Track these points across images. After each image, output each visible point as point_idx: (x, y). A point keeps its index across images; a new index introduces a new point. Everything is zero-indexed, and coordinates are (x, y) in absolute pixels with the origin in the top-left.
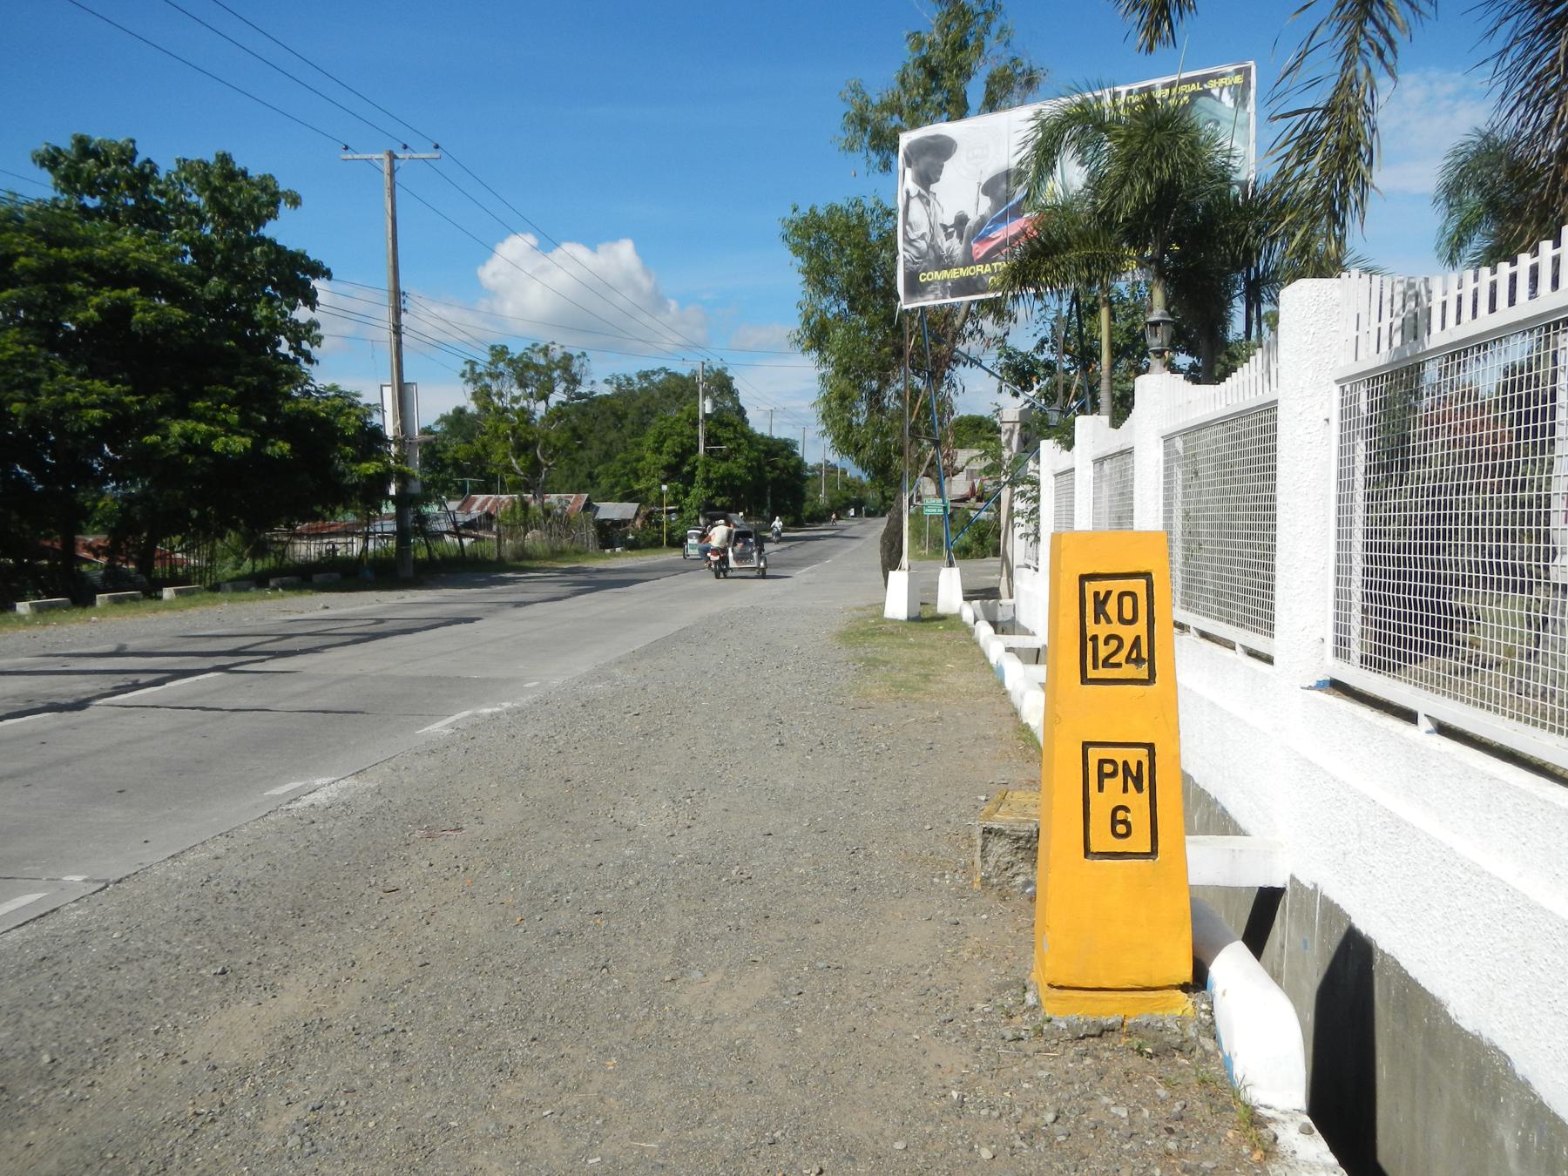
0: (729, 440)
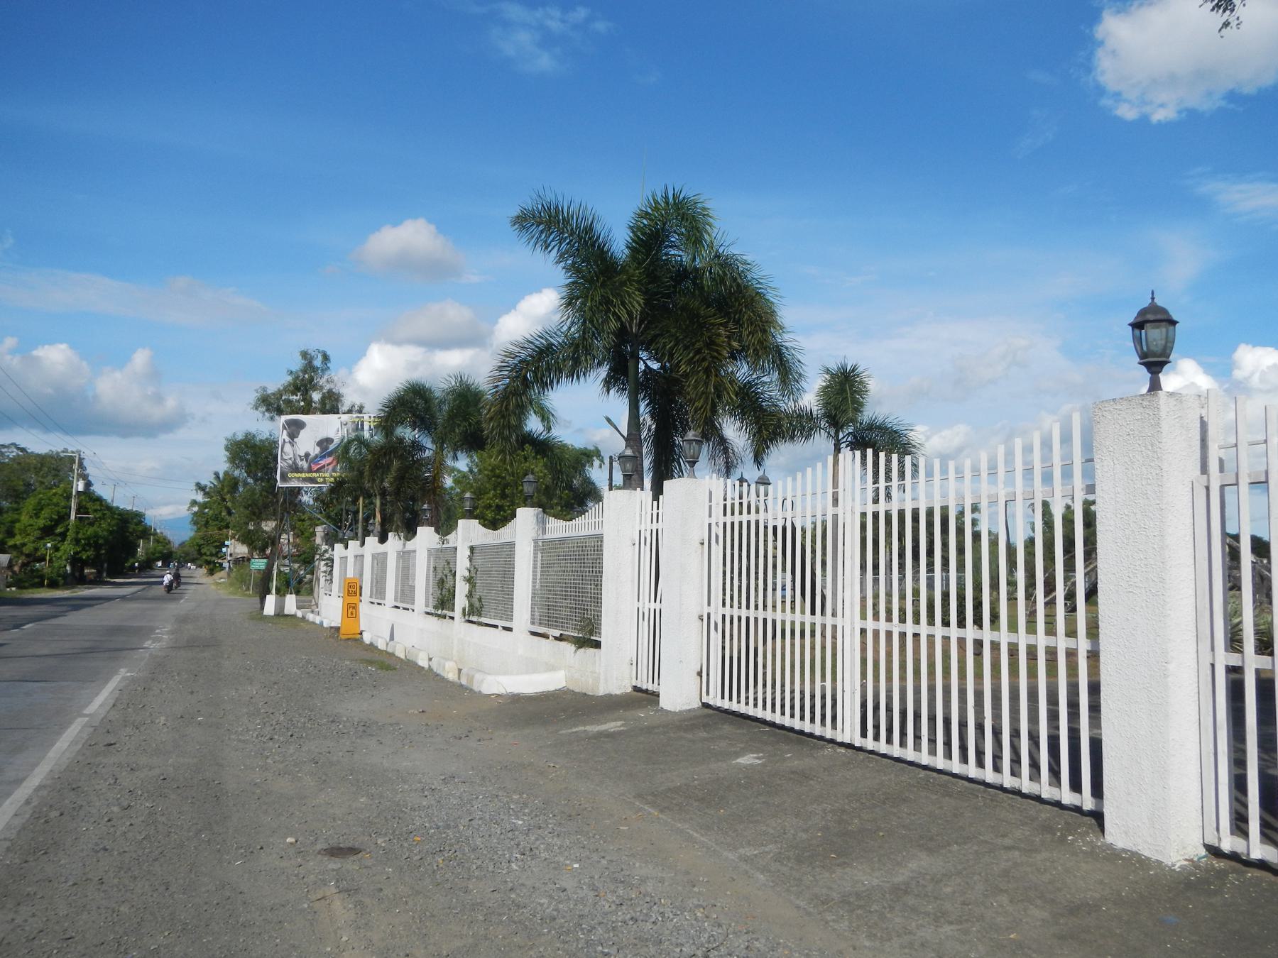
0: (96, 511)
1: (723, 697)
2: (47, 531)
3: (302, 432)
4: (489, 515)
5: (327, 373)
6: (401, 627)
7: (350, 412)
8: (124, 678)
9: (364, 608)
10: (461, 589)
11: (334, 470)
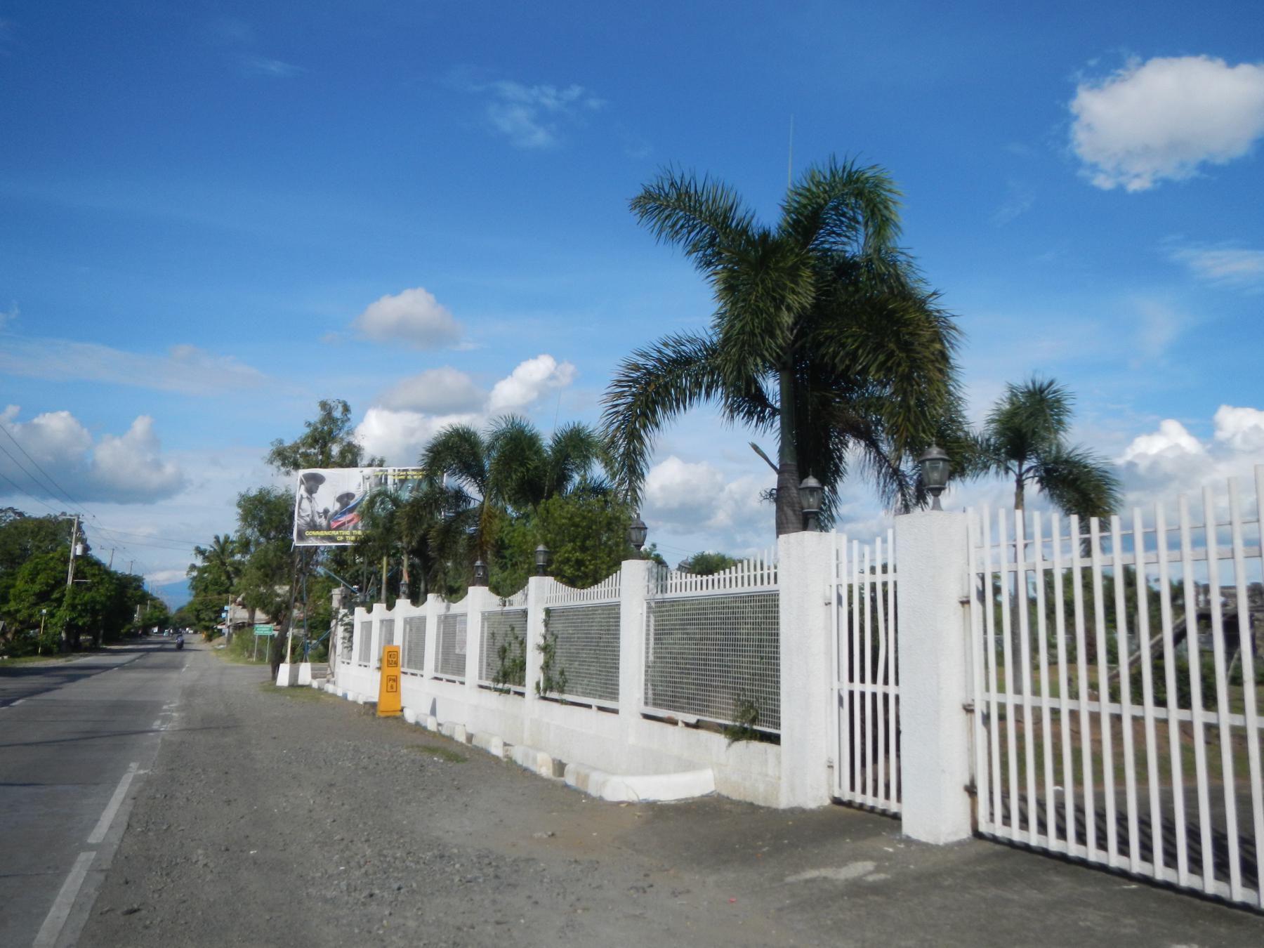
0: (94, 575)
1: (853, 788)
2: (43, 597)
3: (321, 487)
4: (568, 571)
5: (347, 424)
6: (456, 705)
7: (370, 465)
8: (137, 779)
9: (406, 683)
10: (534, 661)
11: (355, 528)
